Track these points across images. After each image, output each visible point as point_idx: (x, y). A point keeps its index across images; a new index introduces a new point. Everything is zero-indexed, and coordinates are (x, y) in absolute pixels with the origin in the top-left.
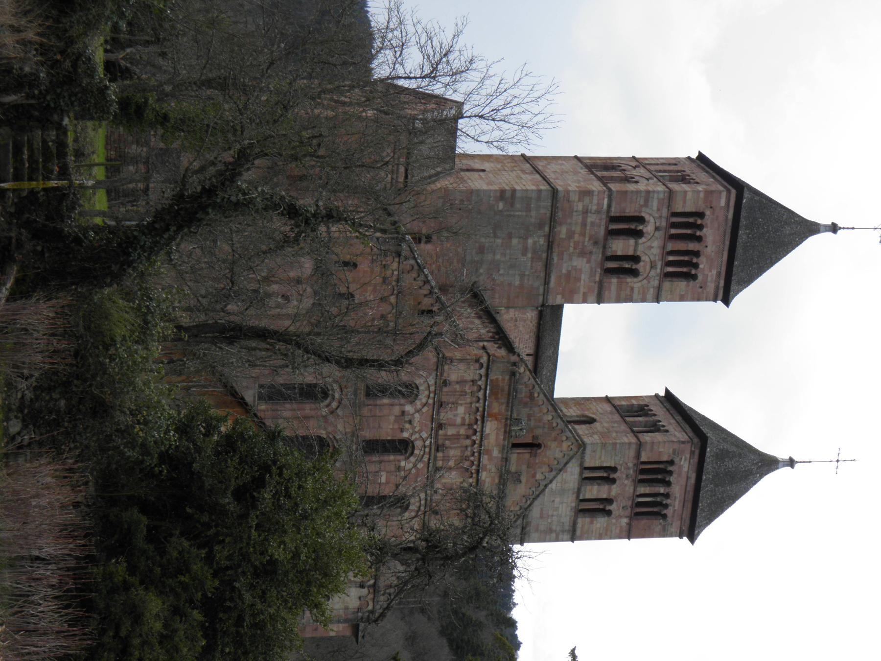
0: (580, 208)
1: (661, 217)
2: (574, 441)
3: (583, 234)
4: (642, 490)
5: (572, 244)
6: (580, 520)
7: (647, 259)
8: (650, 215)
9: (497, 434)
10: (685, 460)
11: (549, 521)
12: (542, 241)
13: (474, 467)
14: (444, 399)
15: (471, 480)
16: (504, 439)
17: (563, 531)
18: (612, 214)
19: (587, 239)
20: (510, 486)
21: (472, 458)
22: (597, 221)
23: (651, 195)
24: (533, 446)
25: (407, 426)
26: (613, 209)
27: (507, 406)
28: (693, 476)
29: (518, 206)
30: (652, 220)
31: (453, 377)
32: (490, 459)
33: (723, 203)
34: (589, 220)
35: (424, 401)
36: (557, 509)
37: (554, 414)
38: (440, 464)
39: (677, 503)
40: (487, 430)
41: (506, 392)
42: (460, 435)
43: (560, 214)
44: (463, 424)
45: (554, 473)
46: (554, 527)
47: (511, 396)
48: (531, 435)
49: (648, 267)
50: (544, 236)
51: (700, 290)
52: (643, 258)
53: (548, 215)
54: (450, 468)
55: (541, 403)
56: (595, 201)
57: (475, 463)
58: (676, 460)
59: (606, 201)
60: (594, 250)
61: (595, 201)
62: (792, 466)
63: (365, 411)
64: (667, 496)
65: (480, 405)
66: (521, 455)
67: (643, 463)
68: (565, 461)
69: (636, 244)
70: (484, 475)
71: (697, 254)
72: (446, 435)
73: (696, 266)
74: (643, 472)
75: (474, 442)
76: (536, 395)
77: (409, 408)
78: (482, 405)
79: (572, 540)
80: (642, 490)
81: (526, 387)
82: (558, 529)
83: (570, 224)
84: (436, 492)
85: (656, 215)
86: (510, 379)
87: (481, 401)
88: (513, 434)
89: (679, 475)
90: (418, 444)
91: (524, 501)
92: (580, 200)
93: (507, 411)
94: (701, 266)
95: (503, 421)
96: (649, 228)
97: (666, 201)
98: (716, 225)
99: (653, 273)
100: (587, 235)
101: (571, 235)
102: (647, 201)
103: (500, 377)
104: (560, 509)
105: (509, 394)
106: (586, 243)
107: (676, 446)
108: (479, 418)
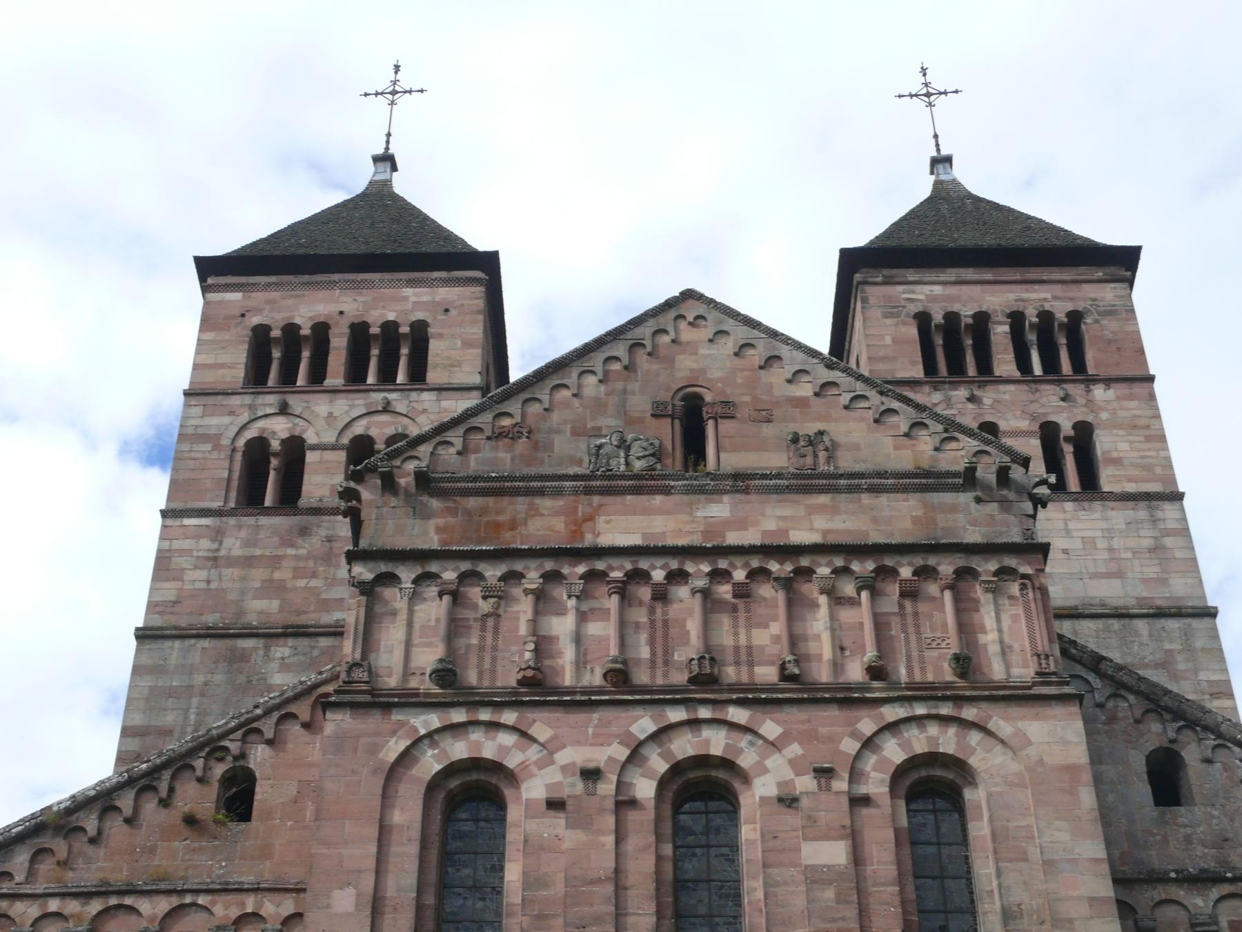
0: (202, 574)
1: (251, 407)
2: (672, 314)
3: (275, 562)
4: (1005, 364)
5: (301, 583)
7: (364, 422)
8: (243, 428)
9: (647, 512)
10: (913, 292)
11: (1129, 555)
12: (282, 650)
13: (774, 566)
15: (824, 571)
16: (667, 491)
17: (1154, 521)
18: (232, 505)
19: (291, 551)
20: (846, 462)
22: (244, 533)
23: (190, 431)
24: (692, 417)
25: (607, 788)
26: (216, 504)
27: (541, 492)
28: (951, 274)
29: (170, 719)
30: (260, 424)
31: (428, 657)
32: (742, 524)
33: (237, 296)
34: (237, 552)
36: (1089, 542)
38: (767, 673)
39: (1034, 296)
40: (633, 540)
41: (491, 501)
43: (210, 619)
45: (784, 351)
46: (1146, 543)
47: (499, 487)
48: (654, 422)
49: (384, 418)
50: (267, 648)
51: (453, 312)
52: (358, 429)
53: (206, 643)
54: (776, 639)
56: (187, 544)
57: (755, 563)
58: (914, 308)
59: (187, 521)
60: (323, 532)
61: (187, 544)
62: (948, 160)
64: (1016, 319)
66: (725, 442)
67: (930, 367)
69: (315, 448)
70: (800, 536)
71: (359, 332)
72: (653, 662)
73: (390, 328)
74: (957, 368)
78: (533, 564)
79: (1178, 497)
80: (1005, 364)
82: (1147, 532)
83: (243, 593)
85: (245, 417)
87: (519, 566)
88: (638, 465)
89: (956, 299)
90: (684, 746)
91: (893, 419)
93: (558, 493)
94: (391, 316)
95: (596, 499)
96: (279, 428)
97: (210, 400)
98: (290, 302)
99: (401, 407)
100: (280, 552)
101: (273, 588)
102: (204, 438)
103: (432, 523)
104: (1086, 534)
106: (304, 552)
107: (876, 313)
108: (581, 569)
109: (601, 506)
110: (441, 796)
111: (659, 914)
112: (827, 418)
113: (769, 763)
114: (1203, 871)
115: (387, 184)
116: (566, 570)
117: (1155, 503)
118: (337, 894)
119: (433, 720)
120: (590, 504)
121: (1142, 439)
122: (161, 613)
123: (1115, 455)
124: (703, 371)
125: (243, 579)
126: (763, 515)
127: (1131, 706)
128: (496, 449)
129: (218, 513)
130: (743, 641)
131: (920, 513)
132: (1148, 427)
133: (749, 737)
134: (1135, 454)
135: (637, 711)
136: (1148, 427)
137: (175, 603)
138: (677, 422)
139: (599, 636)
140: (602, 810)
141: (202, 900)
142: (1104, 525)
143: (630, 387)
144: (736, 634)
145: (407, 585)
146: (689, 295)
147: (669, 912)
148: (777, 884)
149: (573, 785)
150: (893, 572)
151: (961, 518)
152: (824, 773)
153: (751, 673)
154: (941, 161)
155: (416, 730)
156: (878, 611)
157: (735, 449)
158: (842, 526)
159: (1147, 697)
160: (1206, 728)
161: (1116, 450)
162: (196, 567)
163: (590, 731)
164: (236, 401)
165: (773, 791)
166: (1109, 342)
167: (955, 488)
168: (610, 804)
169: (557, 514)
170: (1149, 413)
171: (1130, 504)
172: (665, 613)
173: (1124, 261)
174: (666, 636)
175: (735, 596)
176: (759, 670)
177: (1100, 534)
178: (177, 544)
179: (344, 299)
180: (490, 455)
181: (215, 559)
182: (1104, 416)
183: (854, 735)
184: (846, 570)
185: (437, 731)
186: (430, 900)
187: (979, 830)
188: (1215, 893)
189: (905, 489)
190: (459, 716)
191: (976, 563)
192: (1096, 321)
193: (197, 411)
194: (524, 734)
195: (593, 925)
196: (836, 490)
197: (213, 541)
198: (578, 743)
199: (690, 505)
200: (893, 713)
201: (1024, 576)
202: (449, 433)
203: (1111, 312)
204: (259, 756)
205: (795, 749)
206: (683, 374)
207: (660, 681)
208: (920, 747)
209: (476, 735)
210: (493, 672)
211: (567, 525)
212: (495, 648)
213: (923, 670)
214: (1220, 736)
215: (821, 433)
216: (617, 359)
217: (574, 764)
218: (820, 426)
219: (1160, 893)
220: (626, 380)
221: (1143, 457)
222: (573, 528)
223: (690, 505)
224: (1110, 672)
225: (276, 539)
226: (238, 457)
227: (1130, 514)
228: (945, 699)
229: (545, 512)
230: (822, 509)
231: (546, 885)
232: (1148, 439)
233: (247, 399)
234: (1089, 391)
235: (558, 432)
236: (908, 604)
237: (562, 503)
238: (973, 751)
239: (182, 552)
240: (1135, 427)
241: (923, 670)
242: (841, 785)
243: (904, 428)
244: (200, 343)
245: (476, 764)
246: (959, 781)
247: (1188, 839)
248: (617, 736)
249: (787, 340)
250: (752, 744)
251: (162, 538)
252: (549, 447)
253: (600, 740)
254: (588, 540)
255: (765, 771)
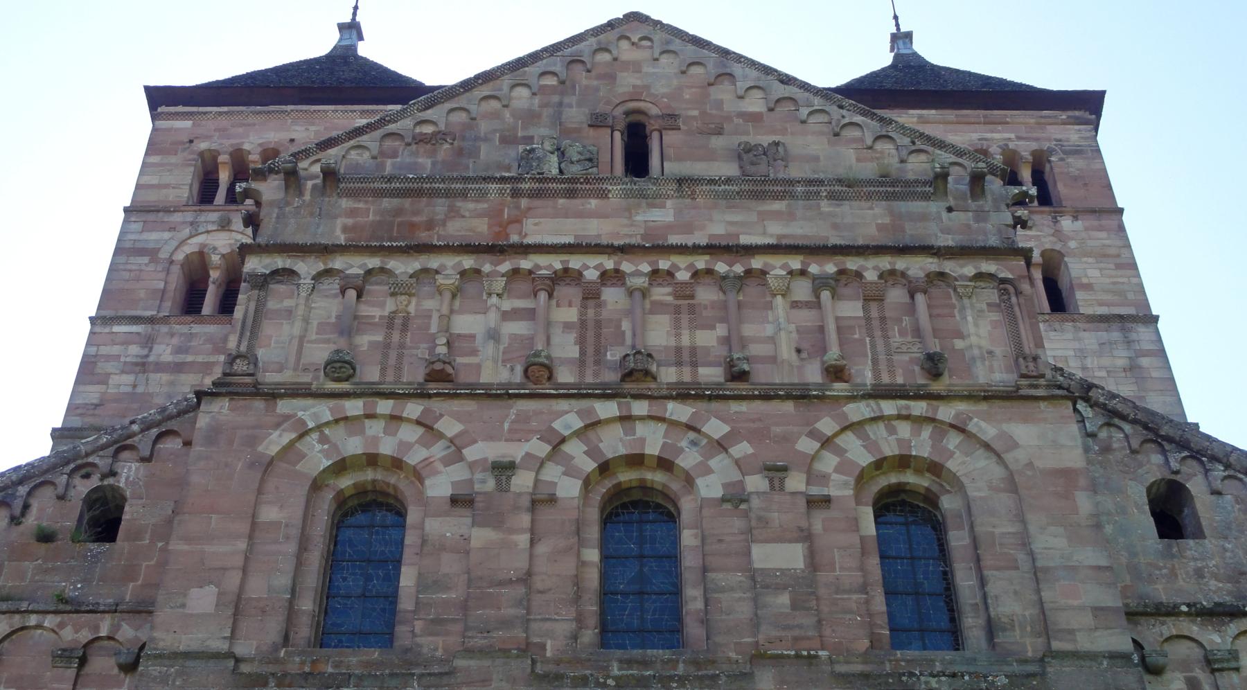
0: (128, 379)
6: (1085, 310)
8: (183, 243)
9: (580, 215)
11: (1104, 374)
13: (721, 267)
14: (414, 374)
16: (603, 195)
21: (683, 276)
22: (175, 341)
23: (128, 245)
25: (522, 481)
26: (149, 313)
27: (464, 195)
30: (200, 239)
32: (689, 229)
33: (188, 124)
35: (409, 433)
37: (506, 82)
38: (711, 374)
41: (407, 203)
42: (583, 323)
44: (530, 314)
45: (737, 69)
46: (1121, 362)
47: (416, 190)
54: (726, 341)
55: (460, 117)
56: (116, 350)
59: (116, 329)
61: (116, 350)
62: (909, 36)
63: (433, 645)
65: (450, 264)
66: (669, 152)
68: (690, 47)
72: (582, 362)
75: (612, 277)
76: (428, 129)
77: (440, 486)
81: (394, 155)
84: (836, 373)
85: (187, 232)
86: (353, 194)
87: (434, 262)
88: (575, 170)
90: (614, 443)
91: (855, 133)
92: (106, 383)
93: (483, 195)
95: (524, 202)
97: (151, 217)
98: (241, 130)
103: (340, 222)
105: (419, 193)
108: (505, 267)
109: (529, 209)
110: (326, 501)
111: (580, 620)
112: (784, 132)
113: (713, 463)
114: (1217, 604)
115: (353, 48)
116: (487, 268)
117: (1129, 325)
118: (194, 592)
119: (324, 410)
120: (518, 207)
121: (1112, 266)
122: (81, 415)
123: (1085, 281)
124: (647, 87)
125: (172, 383)
126: (711, 220)
127: (1127, 437)
128: (416, 154)
129: (151, 320)
130: (685, 341)
131: (887, 220)
132: (1118, 256)
133: (692, 435)
134: (1108, 281)
135: (563, 405)
136: (1118, 256)
137: (97, 406)
138: (617, 135)
139: (521, 335)
140: (516, 508)
141: (49, 621)
142: (1076, 345)
143: (566, 100)
144: (678, 335)
145: (307, 281)
146: (635, 18)
147: (592, 621)
148: (722, 590)
149: (483, 482)
150: (858, 275)
151: (933, 227)
152: (776, 472)
153: (695, 374)
154: (901, 38)
155: (304, 423)
156: (839, 314)
157: (679, 158)
158: (799, 231)
159: (1146, 427)
160: (1214, 459)
161: (1086, 276)
162: (123, 372)
163: (506, 426)
164: (177, 218)
165: (718, 493)
166: (1075, 179)
167: (926, 197)
168: (525, 502)
169: (480, 215)
170: (1119, 243)
171: (1102, 325)
172: (597, 314)
173: (1087, 105)
174: (598, 336)
175: (677, 297)
176: (702, 371)
177: (1072, 353)
178: (104, 350)
179: (297, 128)
180: (408, 160)
181: (144, 364)
182: (1072, 244)
183: (813, 434)
184: (803, 273)
185: (327, 424)
186: (307, 604)
187: (957, 540)
188: (1233, 628)
189: (869, 196)
190: (354, 407)
191: (949, 267)
192: (1062, 160)
193: (137, 227)
194: (429, 428)
195: (497, 629)
196: (793, 196)
197: (143, 347)
198: (490, 438)
199: (628, 210)
200: (858, 411)
201: (1004, 281)
202: (365, 137)
203: (1077, 152)
204: (129, 472)
205: (742, 449)
206: (626, 89)
207: (589, 379)
208: (890, 449)
209: (374, 428)
210: (399, 368)
211: (489, 227)
212: (402, 346)
213: (892, 373)
214: (1228, 466)
215: (777, 144)
216: (554, 74)
217: (485, 460)
218: (776, 138)
219: (1170, 627)
220: (563, 93)
221: (1114, 283)
222: (497, 229)
223: (628, 210)
224: (1102, 400)
225: (209, 346)
226: (176, 269)
227: (1104, 336)
228: (917, 397)
229: (467, 214)
230: (777, 215)
231: (447, 589)
232: (1119, 266)
233: (189, 217)
234: (1056, 221)
235: (486, 139)
236: (874, 307)
237: (486, 206)
238: (952, 454)
239: (108, 358)
240: (1105, 256)
241: (892, 373)
242: (796, 482)
243: (869, 142)
244: (145, 165)
245: (372, 460)
246: (935, 488)
247: (1199, 573)
248: (536, 432)
249: (739, 58)
250: (694, 443)
251: (89, 344)
252: (474, 153)
253: (517, 435)
254: (514, 238)
255: (709, 471)
